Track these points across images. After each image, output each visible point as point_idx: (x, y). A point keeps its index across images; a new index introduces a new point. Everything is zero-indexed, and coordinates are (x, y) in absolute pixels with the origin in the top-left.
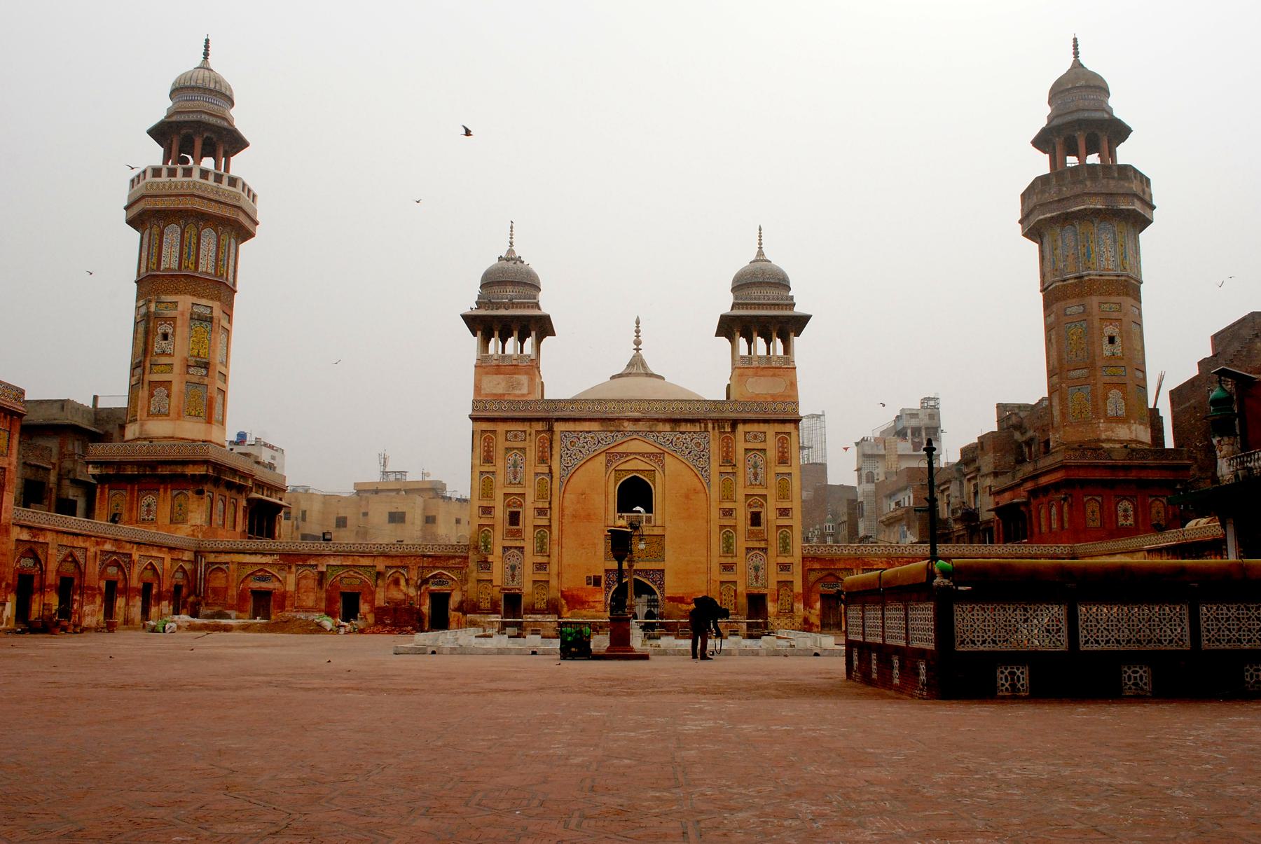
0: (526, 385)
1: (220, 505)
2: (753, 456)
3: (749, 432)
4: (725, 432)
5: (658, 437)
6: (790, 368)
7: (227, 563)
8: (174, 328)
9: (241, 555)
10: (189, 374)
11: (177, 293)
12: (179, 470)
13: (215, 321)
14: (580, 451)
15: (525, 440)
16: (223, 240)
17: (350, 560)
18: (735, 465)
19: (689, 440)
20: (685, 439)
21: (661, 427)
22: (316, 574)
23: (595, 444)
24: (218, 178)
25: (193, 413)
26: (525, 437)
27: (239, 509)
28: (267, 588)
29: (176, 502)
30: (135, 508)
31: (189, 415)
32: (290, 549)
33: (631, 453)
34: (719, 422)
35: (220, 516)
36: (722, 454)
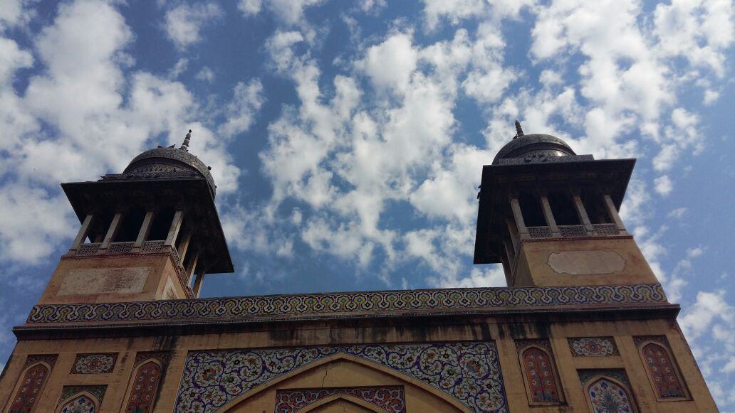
0: (142, 282)
2: (598, 385)
3: (578, 339)
4: (526, 340)
5: (388, 354)
6: (625, 238)
14: (222, 389)
15: (111, 370)
18: (565, 404)
19: (453, 357)
20: (446, 356)
21: (393, 336)
23: (256, 373)
26: (113, 367)
33: (332, 389)
34: (513, 321)
36: (530, 383)
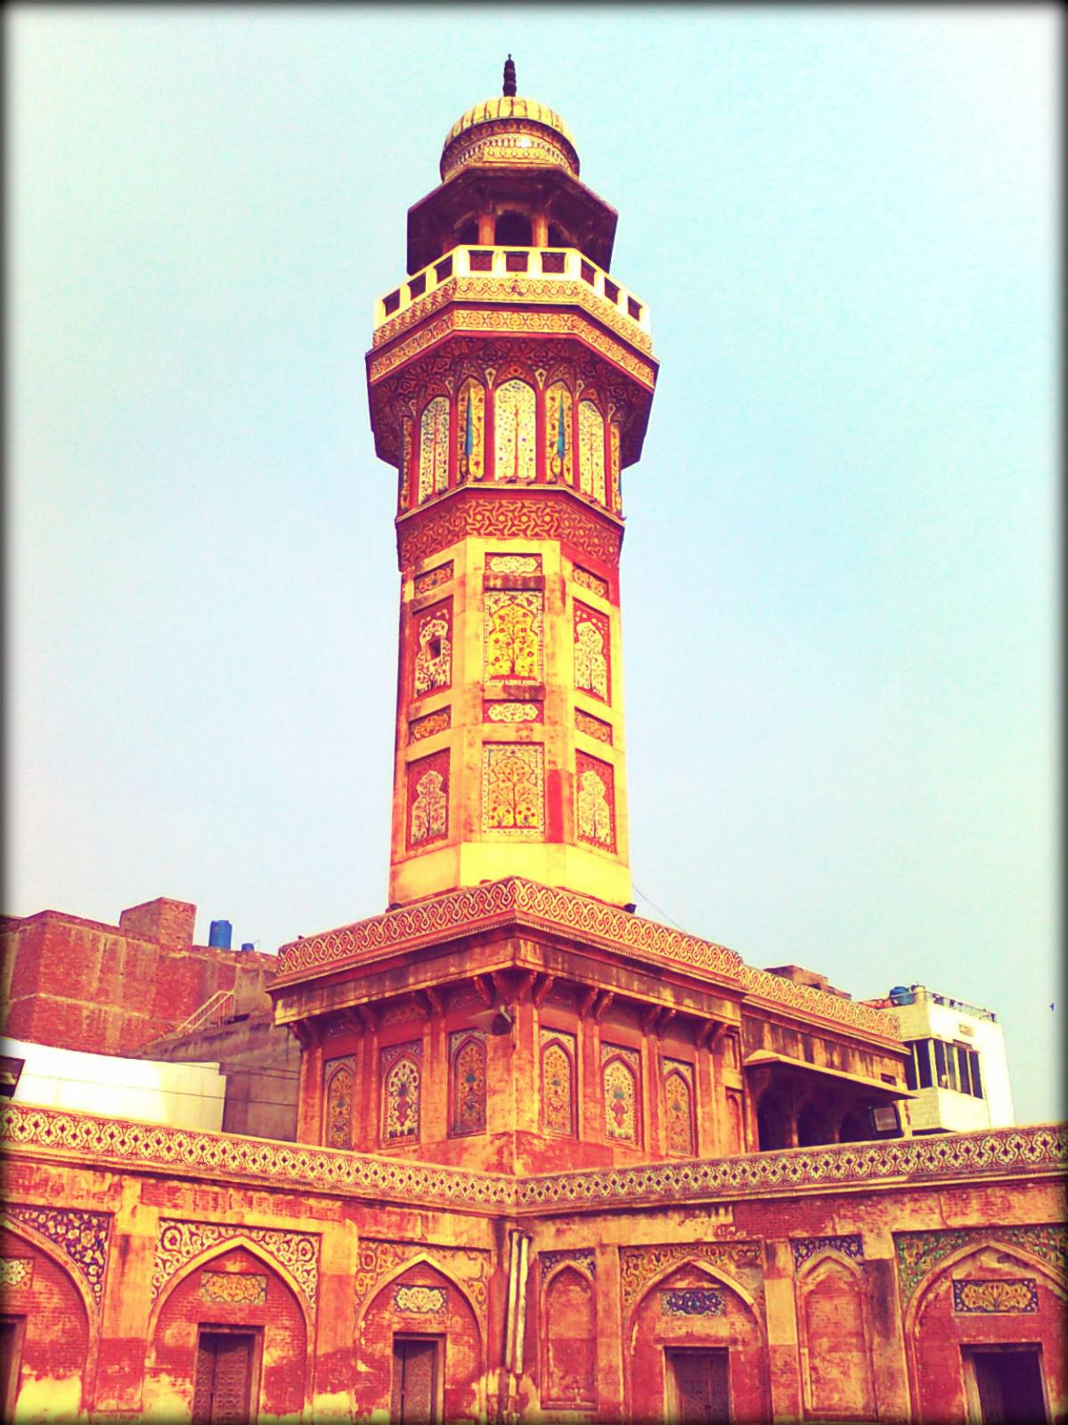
1: (618, 1077)
7: (589, 1252)
8: (450, 622)
9: (625, 1221)
10: (491, 721)
11: (450, 543)
12: (453, 970)
13: (549, 585)
16: (553, 399)
17: (975, 1204)
22: (858, 1271)
24: (517, 263)
25: (509, 820)
27: (707, 1092)
28: (708, 1338)
29: (460, 1069)
30: (373, 1105)
31: (499, 826)
32: (764, 1183)
35: (619, 1110)
